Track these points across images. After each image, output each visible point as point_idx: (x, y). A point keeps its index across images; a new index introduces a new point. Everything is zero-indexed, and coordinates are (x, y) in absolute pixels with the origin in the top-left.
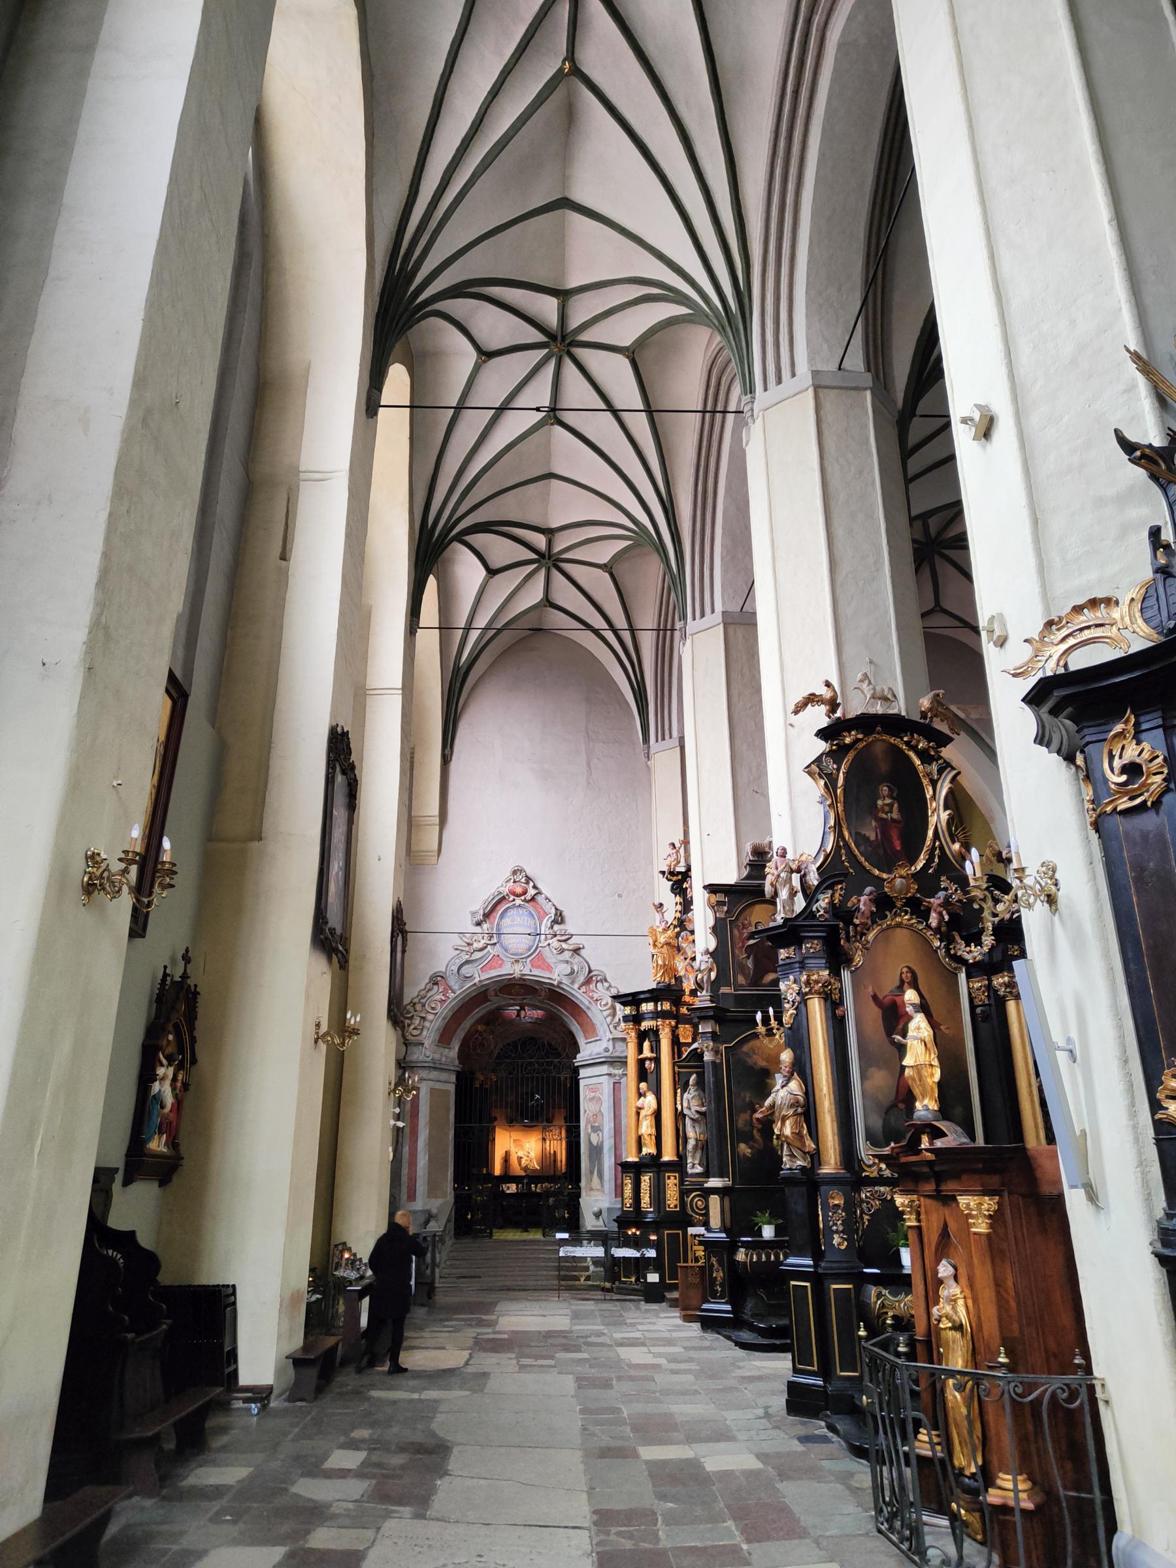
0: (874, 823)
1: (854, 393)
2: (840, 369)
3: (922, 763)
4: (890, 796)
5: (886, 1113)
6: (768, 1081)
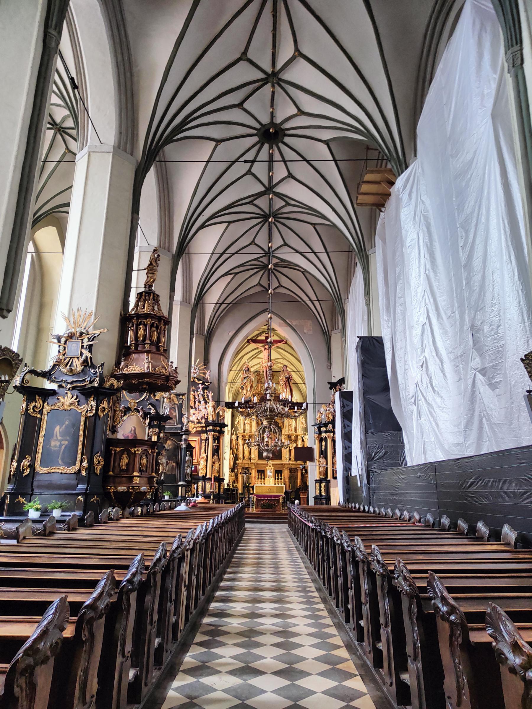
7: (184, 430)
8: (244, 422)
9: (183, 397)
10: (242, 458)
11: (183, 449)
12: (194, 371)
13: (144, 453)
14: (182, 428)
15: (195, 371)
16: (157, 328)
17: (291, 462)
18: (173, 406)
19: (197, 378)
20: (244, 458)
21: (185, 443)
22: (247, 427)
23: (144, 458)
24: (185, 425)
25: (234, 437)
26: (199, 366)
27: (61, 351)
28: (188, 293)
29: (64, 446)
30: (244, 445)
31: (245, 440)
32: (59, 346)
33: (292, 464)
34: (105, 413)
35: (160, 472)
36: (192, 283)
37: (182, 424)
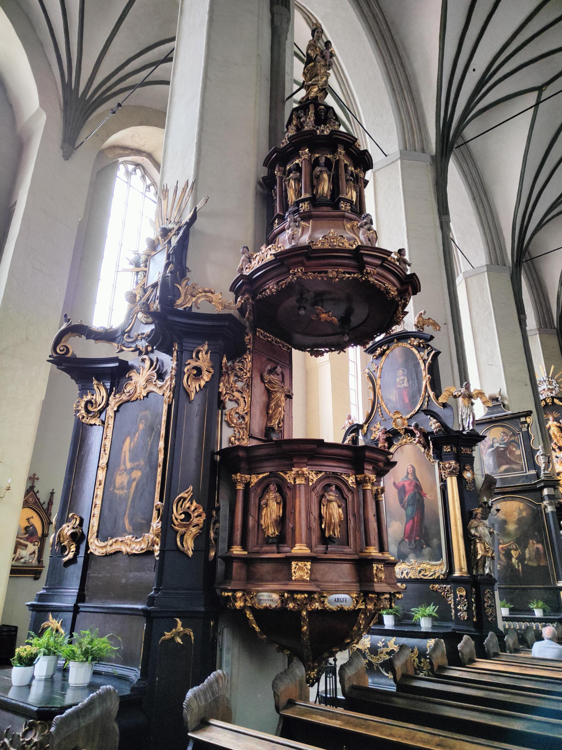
0: (395, 391)
1: (392, 165)
2: (386, 156)
3: (419, 352)
4: (404, 375)
5: (399, 544)
6: (506, 526)
7: (542, 477)
9: (528, 420)
11: (550, 516)
12: (549, 387)
13: (329, 485)
14: (538, 475)
15: (551, 387)
16: (328, 163)
18: (513, 439)
19: (557, 398)
21: (550, 504)
23: (330, 501)
24: (542, 468)
26: (557, 376)
27: (139, 282)
28: (497, 250)
29: (134, 484)
32: (137, 273)
34: (203, 383)
35: (479, 557)
36: (502, 232)
37: (536, 467)
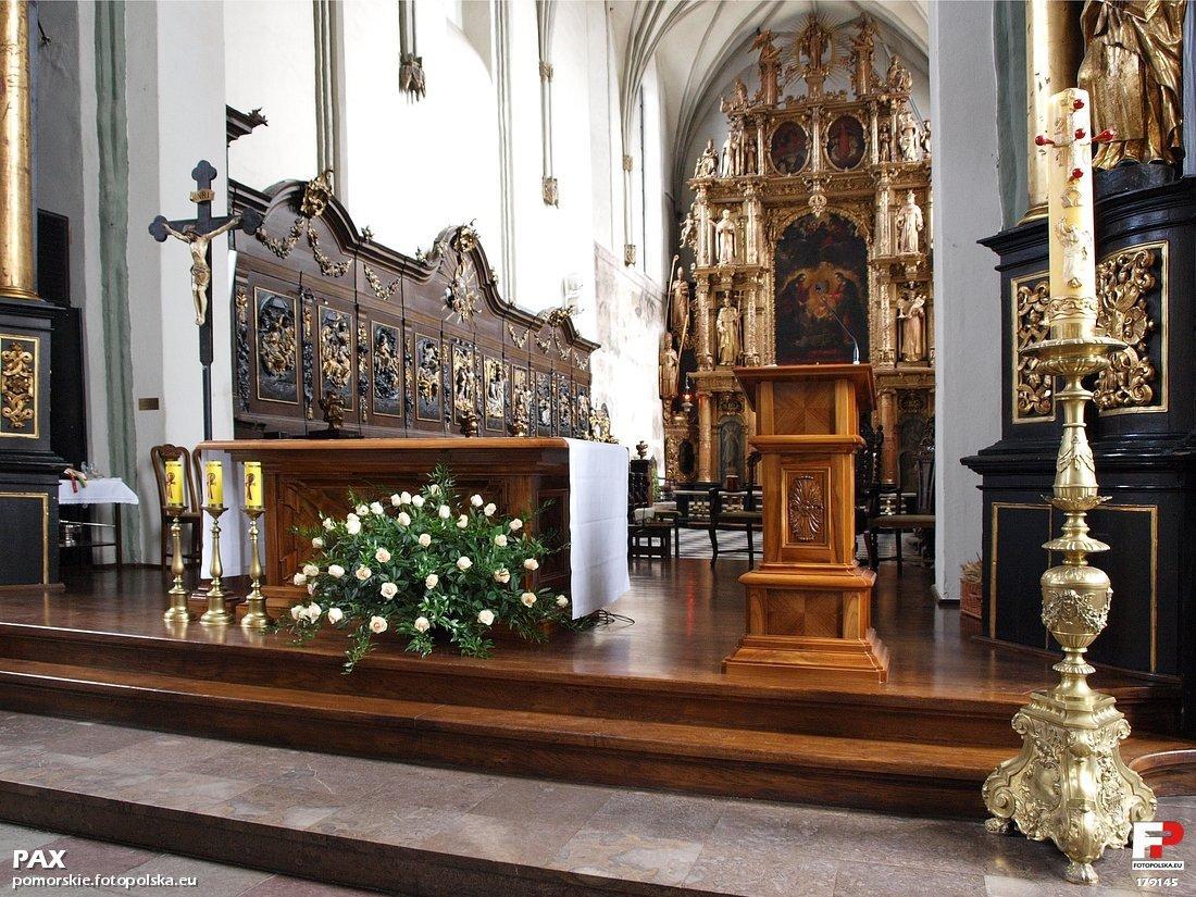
8: (714, 229)
10: (710, 360)
17: (902, 368)
20: (717, 360)
22: (726, 247)
25: (677, 285)
30: (714, 313)
31: (720, 295)
33: (906, 374)
